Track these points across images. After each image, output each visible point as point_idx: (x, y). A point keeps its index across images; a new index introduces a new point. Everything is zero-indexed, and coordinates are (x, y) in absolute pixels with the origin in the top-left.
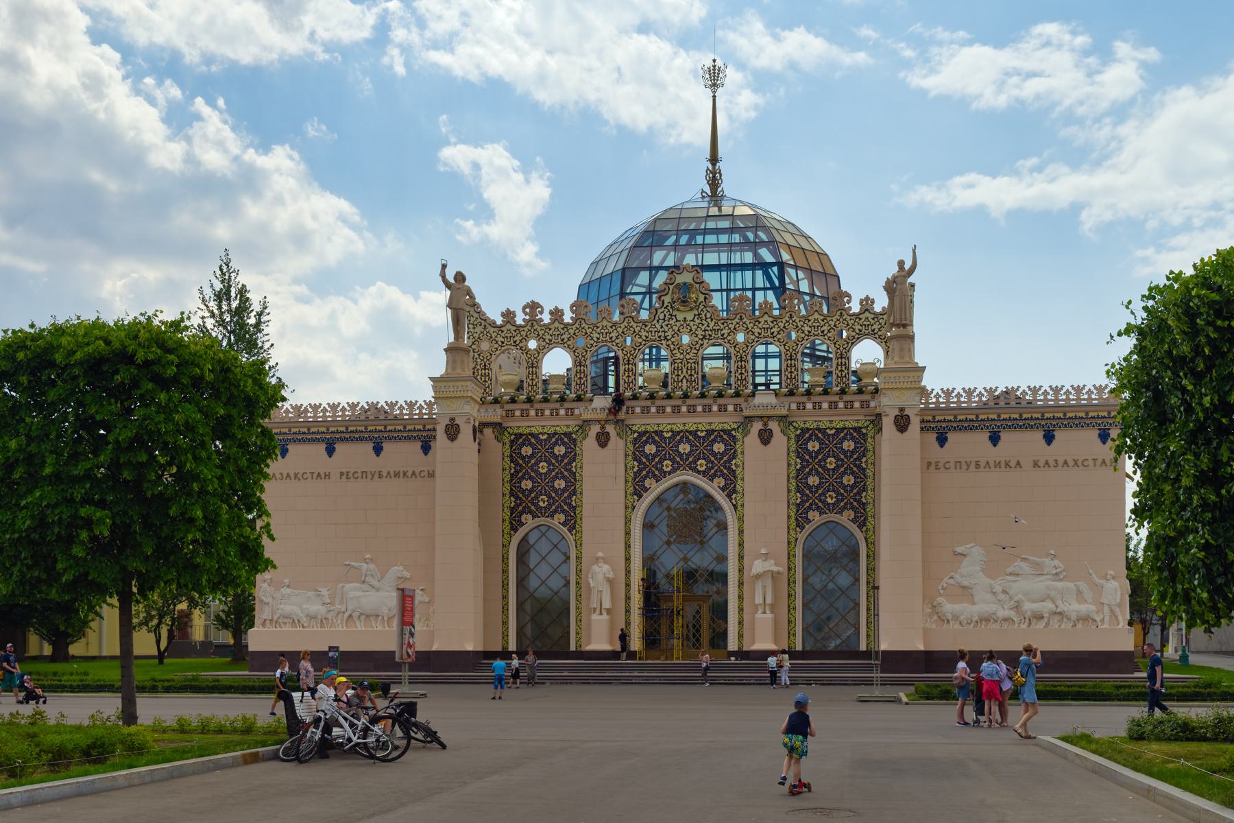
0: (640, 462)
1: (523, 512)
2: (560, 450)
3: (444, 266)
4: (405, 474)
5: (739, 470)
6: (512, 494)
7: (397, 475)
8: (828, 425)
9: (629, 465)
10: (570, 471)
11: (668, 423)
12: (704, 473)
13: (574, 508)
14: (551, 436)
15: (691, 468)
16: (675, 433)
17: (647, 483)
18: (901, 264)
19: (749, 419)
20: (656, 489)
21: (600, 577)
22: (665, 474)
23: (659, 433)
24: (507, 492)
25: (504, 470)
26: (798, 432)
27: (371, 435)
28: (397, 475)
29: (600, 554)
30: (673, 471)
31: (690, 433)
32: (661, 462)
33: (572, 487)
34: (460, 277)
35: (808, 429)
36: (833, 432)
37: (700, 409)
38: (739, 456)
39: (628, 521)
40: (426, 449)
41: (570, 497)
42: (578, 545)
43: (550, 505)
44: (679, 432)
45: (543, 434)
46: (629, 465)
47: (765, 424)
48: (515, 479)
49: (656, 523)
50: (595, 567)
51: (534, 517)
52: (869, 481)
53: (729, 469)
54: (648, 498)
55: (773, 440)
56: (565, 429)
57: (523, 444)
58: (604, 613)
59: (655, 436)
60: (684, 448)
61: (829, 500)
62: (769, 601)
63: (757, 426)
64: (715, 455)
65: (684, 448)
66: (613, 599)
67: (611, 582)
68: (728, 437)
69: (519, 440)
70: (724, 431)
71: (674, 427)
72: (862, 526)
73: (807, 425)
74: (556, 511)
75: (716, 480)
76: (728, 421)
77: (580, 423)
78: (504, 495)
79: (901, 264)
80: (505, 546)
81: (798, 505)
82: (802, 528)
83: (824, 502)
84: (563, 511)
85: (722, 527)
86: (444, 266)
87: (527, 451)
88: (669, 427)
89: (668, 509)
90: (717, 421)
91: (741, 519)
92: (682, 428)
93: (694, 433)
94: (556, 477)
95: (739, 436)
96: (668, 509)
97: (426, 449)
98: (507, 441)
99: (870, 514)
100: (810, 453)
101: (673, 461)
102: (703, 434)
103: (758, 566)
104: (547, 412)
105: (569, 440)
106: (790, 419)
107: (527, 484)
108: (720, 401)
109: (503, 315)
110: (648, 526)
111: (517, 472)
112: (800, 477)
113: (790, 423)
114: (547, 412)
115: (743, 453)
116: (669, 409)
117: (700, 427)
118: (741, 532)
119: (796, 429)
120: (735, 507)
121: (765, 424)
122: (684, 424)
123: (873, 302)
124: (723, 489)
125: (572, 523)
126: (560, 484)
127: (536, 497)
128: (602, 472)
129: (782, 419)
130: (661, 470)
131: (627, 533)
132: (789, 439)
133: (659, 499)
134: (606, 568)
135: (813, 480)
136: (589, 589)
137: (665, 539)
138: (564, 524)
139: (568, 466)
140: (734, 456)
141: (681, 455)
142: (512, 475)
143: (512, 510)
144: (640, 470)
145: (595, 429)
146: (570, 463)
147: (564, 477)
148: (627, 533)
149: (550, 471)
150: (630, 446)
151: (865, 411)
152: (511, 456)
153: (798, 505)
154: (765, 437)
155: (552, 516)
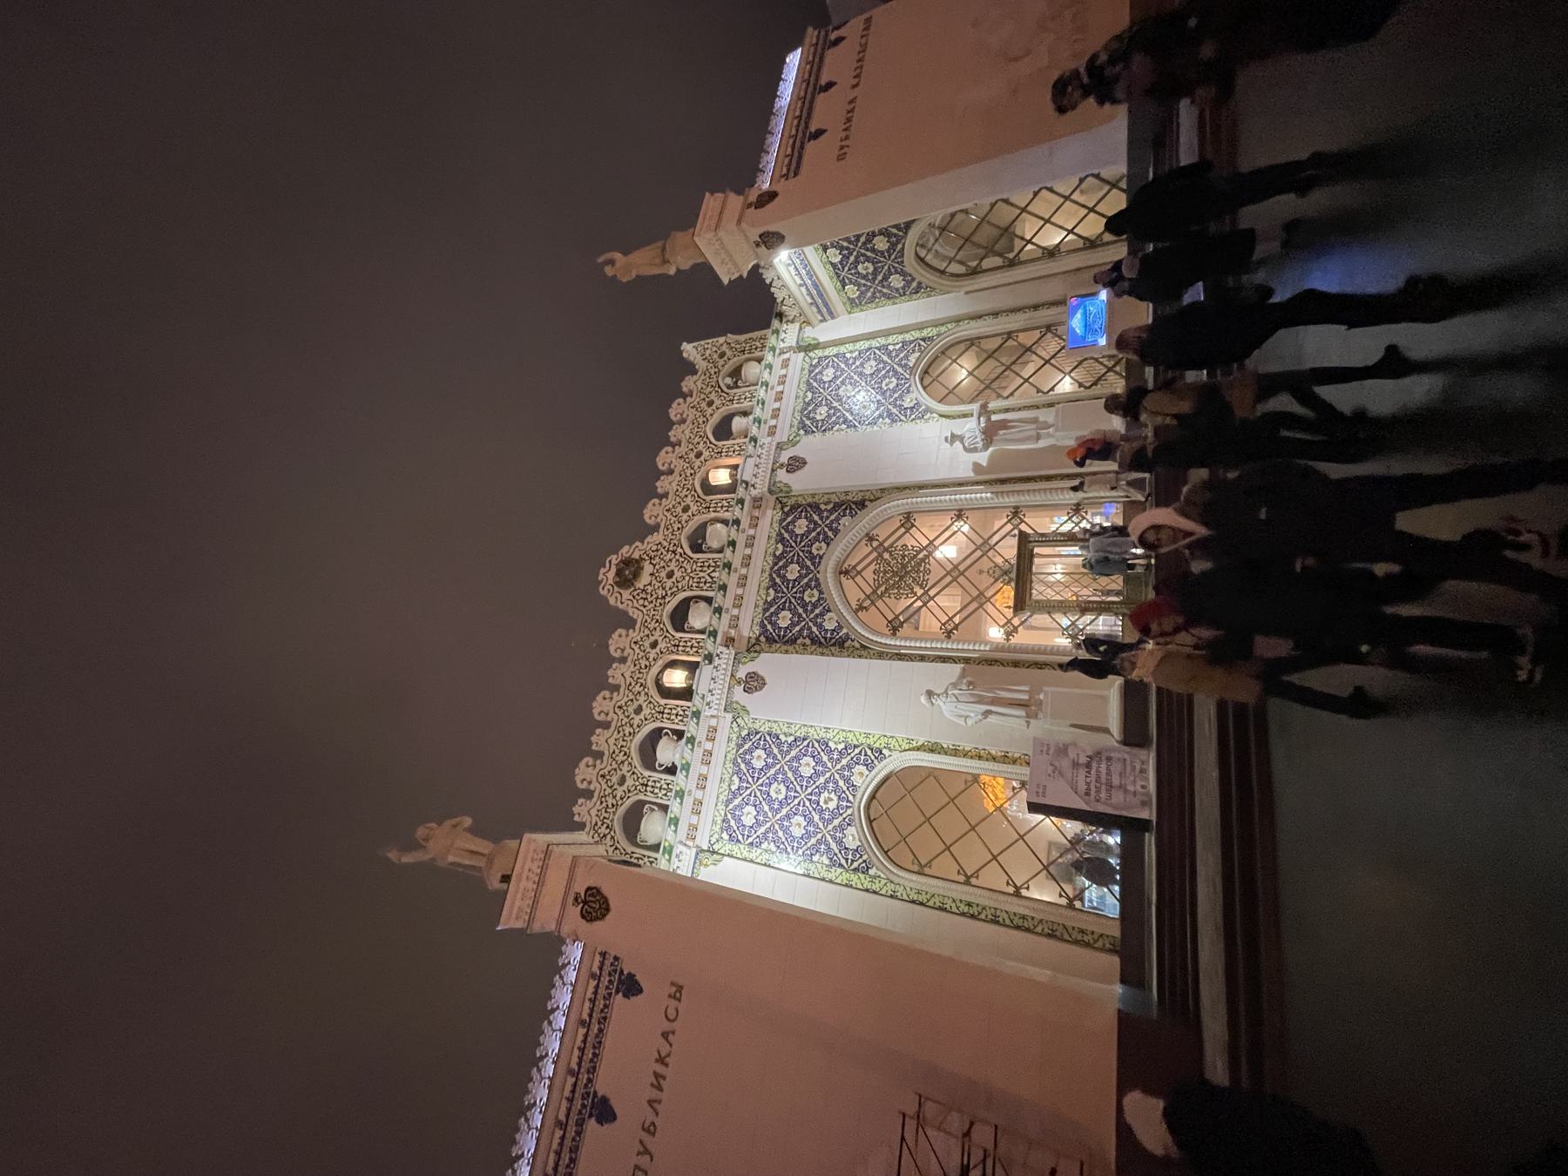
5: (834, 499)
16: (774, 585)
23: (769, 604)
30: (818, 585)
44: (772, 579)
59: (770, 610)
60: (793, 572)
63: (782, 475)
65: (793, 572)
71: (764, 585)
77: (729, 716)
88: (763, 592)
93: (778, 559)
95: (791, 502)
153: (894, 421)
154: (796, 464)
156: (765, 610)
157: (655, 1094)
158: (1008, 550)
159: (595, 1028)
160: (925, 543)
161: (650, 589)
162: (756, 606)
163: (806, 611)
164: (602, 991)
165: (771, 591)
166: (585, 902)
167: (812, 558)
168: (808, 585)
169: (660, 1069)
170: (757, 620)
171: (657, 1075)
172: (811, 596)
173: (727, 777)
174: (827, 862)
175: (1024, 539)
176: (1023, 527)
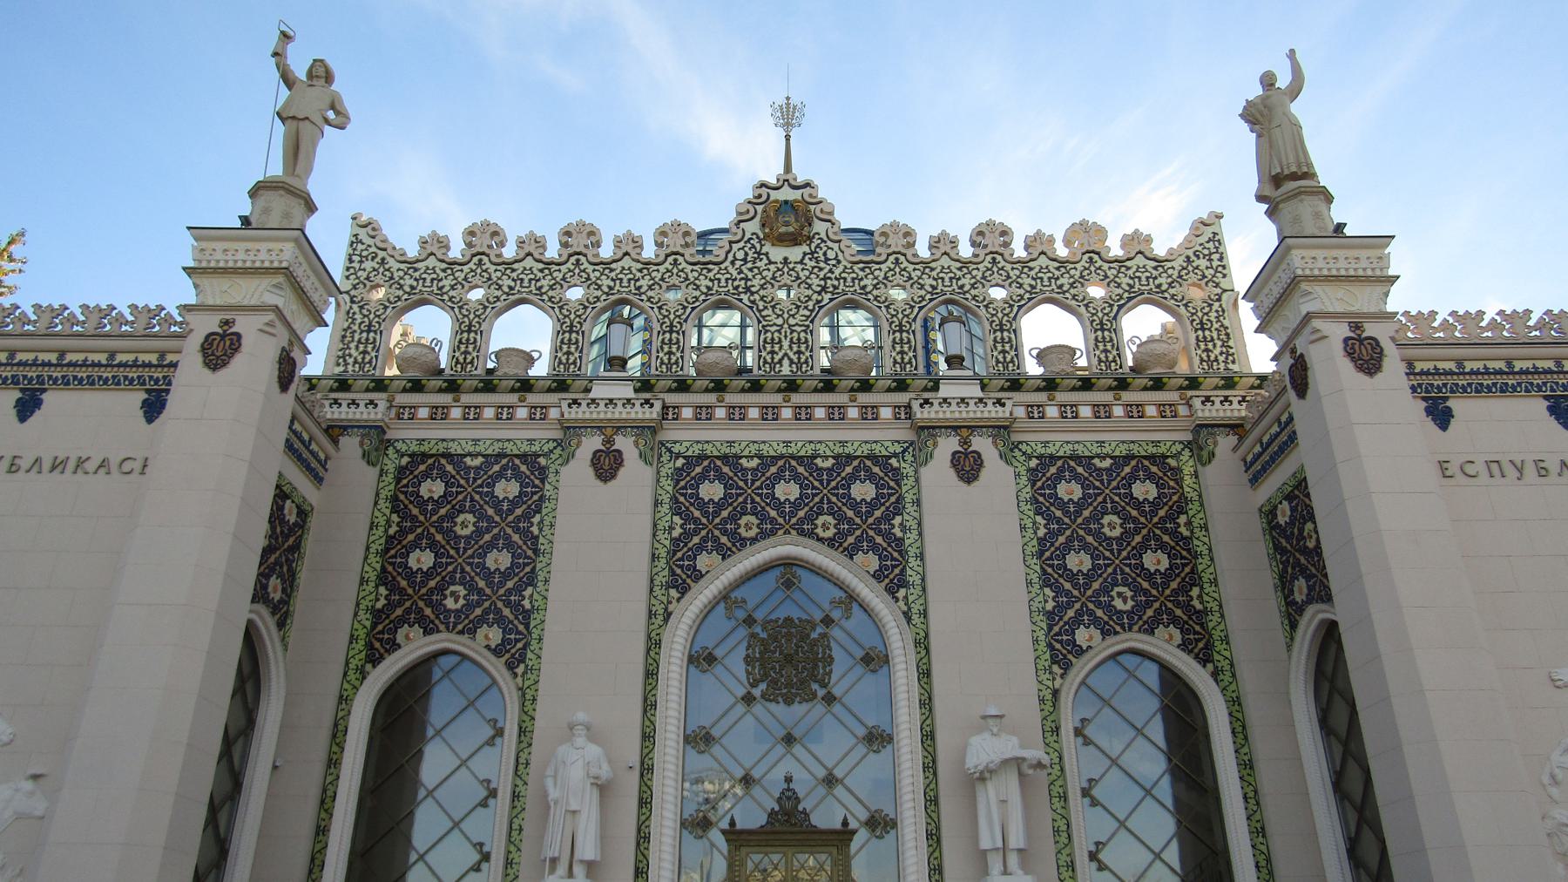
0: (688, 518)
1: (402, 621)
2: (507, 489)
3: (286, 37)
4: (80, 462)
5: (911, 538)
6: (383, 578)
7: (58, 465)
8: (1096, 450)
9: (663, 524)
10: (526, 534)
11: (754, 434)
12: (831, 543)
13: (527, 614)
14: (490, 459)
15: (801, 533)
16: (766, 461)
17: (703, 561)
18: (1268, 81)
19: (928, 430)
20: (720, 574)
21: (576, 774)
22: (742, 543)
24: (372, 576)
25: (373, 526)
26: (1034, 463)
27: (21, 371)
28: (58, 465)
29: (581, 716)
30: (764, 535)
31: (800, 459)
32: (733, 518)
33: (527, 571)
34: (321, 73)
35: (1053, 458)
36: (1107, 463)
37: (820, 413)
38: (910, 508)
39: (653, 644)
40: (154, 407)
41: (519, 589)
42: (527, 700)
43: (470, 606)
44: (775, 459)
45: (473, 455)
46: (663, 524)
47: (965, 442)
48: (394, 548)
49: (718, 653)
50: (562, 750)
51: (427, 632)
52: (1203, 563)
53: (888, 535)
54: (703, 594)
55: (984, 473)
56: (525, 448)
57: (426, 475)
58: (579, 870)
60: (787, 491)
61: (1118, 604)
62: (1016, 840)
63: (948, 445)
64: (855, 505)
65: (787, 491)
66: (604, 838)
67: (604, 789)
68: (881, 468)
69: (422, 462)
70: (872, 457)
71: (766, 450)
72: (1204, 658)
73: (1051, 450)
74: (482, 620)
75: (859, 557)
76: (886, 435)
77: (558, 435)
78: (363, 581)
79: (1268, 81)
80: (344, 700)
81: (1050, 615)
82: (1067, 667)
83: (1109, 608)
84: (500, 620)
85: (875, 660)
86: (286, 37)
87: (433, 488)
88: (753, 449)
89: (749, 621)
90: (857, 437)
91: (923, 644)
92: (782, 450)
93: (808, 461)
94: (492, 545)
95: (907, 469)
96: (749, 621)
97: (154, 407)
98: (391, 467)
99: (1217, 634)
100: (1063, 505)
101: (763, 518)
102: (829, 463)
103: (985, 749)
104: (489, 413)
105: (532, 469)
106: (1016, 437)
107: (422, 559)
108: (864, 398)
109: (423, 243)
110: (702, 659)
111: (403, 532)
112: (1048, 558)
113: (1016, 445)
114: (489, 413)
115: (918, 503)
116: (754, 413)
117: (822, 449)
118: (925, 674)
119: (1030, 457)
120: (908, 616)
121: (965, 442)
122: (787, 443)
123: (1148, 240)
124: (878, 576)
125: (517, 652)
126: (499, 560)
127: (441, 589)
128: (601, 535)
129: (1001, 430)
130: (734, 536)
131: (651, 674)
132: (1017, 475)
133: (725, 597)
134: (594, 751)
135: (1078, 561)
136: (545, 807)
137: (741, 692)
138: (497, 652)
139: (524, 528)
140: (898, 509)
141: (779, 506)
142: (390, 539)
143: (377, 615)
144: (688, 535)
145: (592, 443)
146: (527, 516)
147: (509, 545)
148: (651, 674)
149: (479, 532)
150: (668, 485)
151: (1169, 423)
152: (394, 499)
153: (1050, 615)
154: (967, 467)
155: (472, 632)
156: (725, 458)
157: (47, 465)
158: (826, 816)
159: (107, 374)
160: (837, 691)
161: (761, 264)
162: (731, 443)
163: (724, 521)
164: (146, 373)
165: (756, 462)
166: (223, 336)
167: (811, 518)
168: (763, 518)
169: (71, 465)
170: (709, 449)
171: (65, 462)
172: (748, 525)
173: (481, 448)
174: (379, 605)
175: (843, 835)
176: (862, 836)
